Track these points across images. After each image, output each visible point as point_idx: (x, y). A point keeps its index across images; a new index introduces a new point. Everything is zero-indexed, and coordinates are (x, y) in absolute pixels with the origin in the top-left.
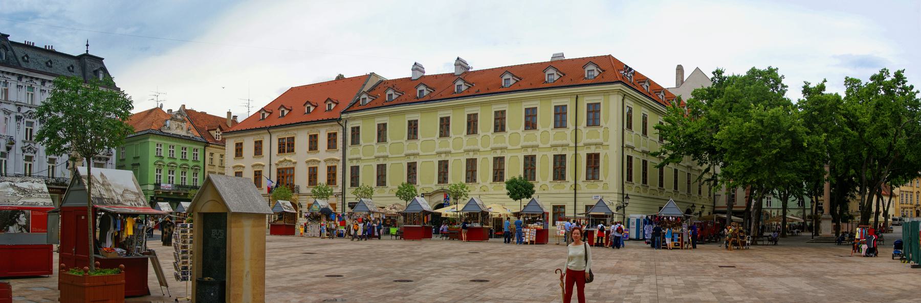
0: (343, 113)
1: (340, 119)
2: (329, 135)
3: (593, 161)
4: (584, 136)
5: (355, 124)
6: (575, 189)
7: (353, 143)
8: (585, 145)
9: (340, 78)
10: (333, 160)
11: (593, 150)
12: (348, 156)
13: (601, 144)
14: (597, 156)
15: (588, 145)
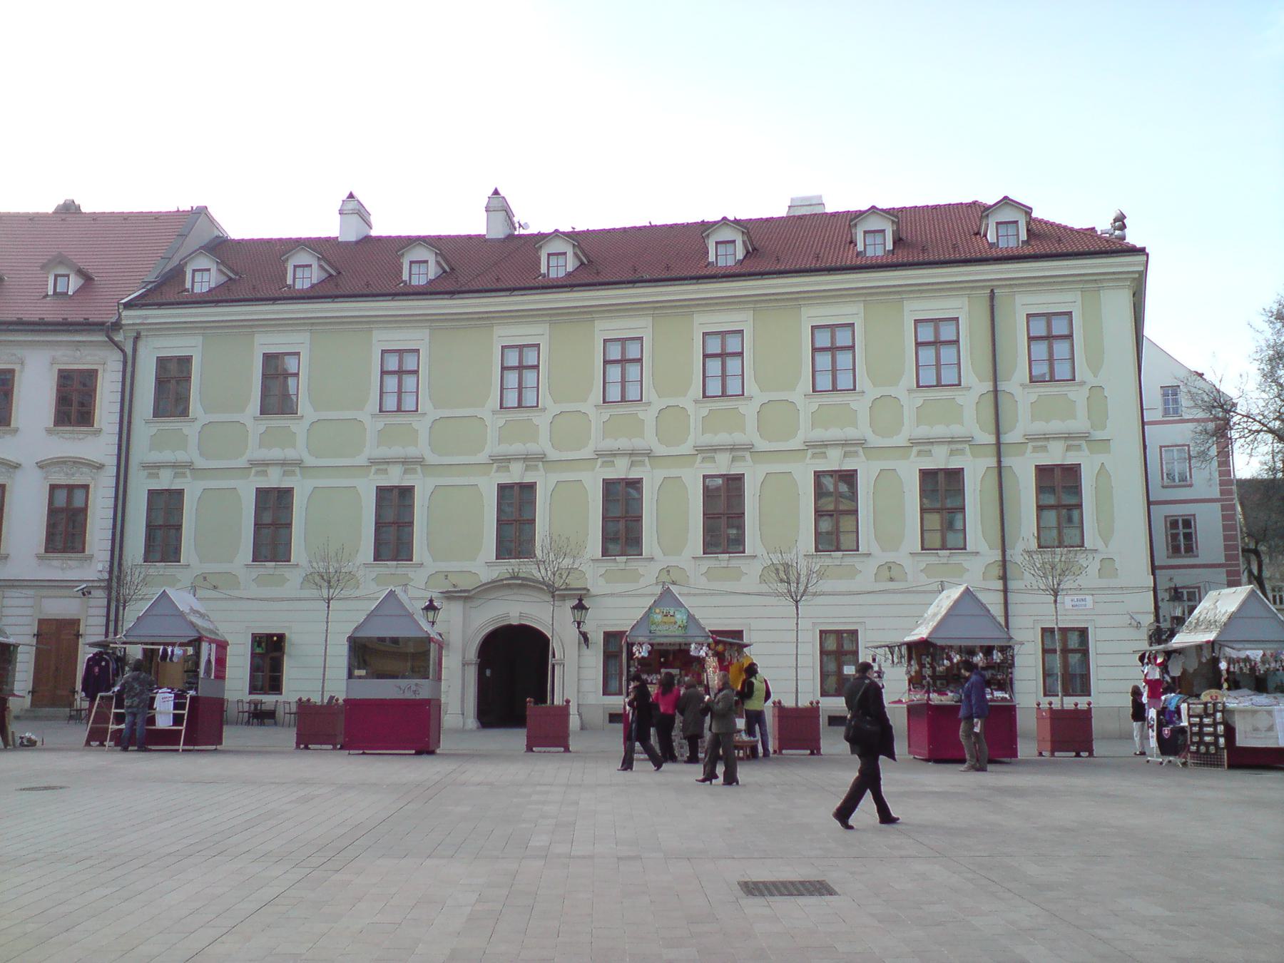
0: (128, 306)
1: (117, 326)
2: (65, 378)
3: (1059, 486)
4: (1023, 411)
5: (174, 346)
6: (1004, 578)
7: (160, 411)
8: (1030, 438)
9: (69, 209)
10: (78, 463)
11: (1056, 455)
12: (141, 451)
13: (1086, 437)
14: (1072, 472)
15: (1041, 440)
